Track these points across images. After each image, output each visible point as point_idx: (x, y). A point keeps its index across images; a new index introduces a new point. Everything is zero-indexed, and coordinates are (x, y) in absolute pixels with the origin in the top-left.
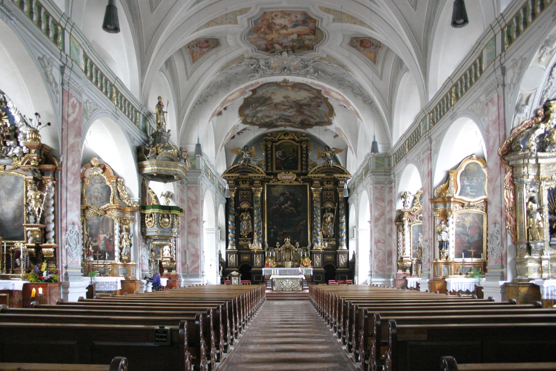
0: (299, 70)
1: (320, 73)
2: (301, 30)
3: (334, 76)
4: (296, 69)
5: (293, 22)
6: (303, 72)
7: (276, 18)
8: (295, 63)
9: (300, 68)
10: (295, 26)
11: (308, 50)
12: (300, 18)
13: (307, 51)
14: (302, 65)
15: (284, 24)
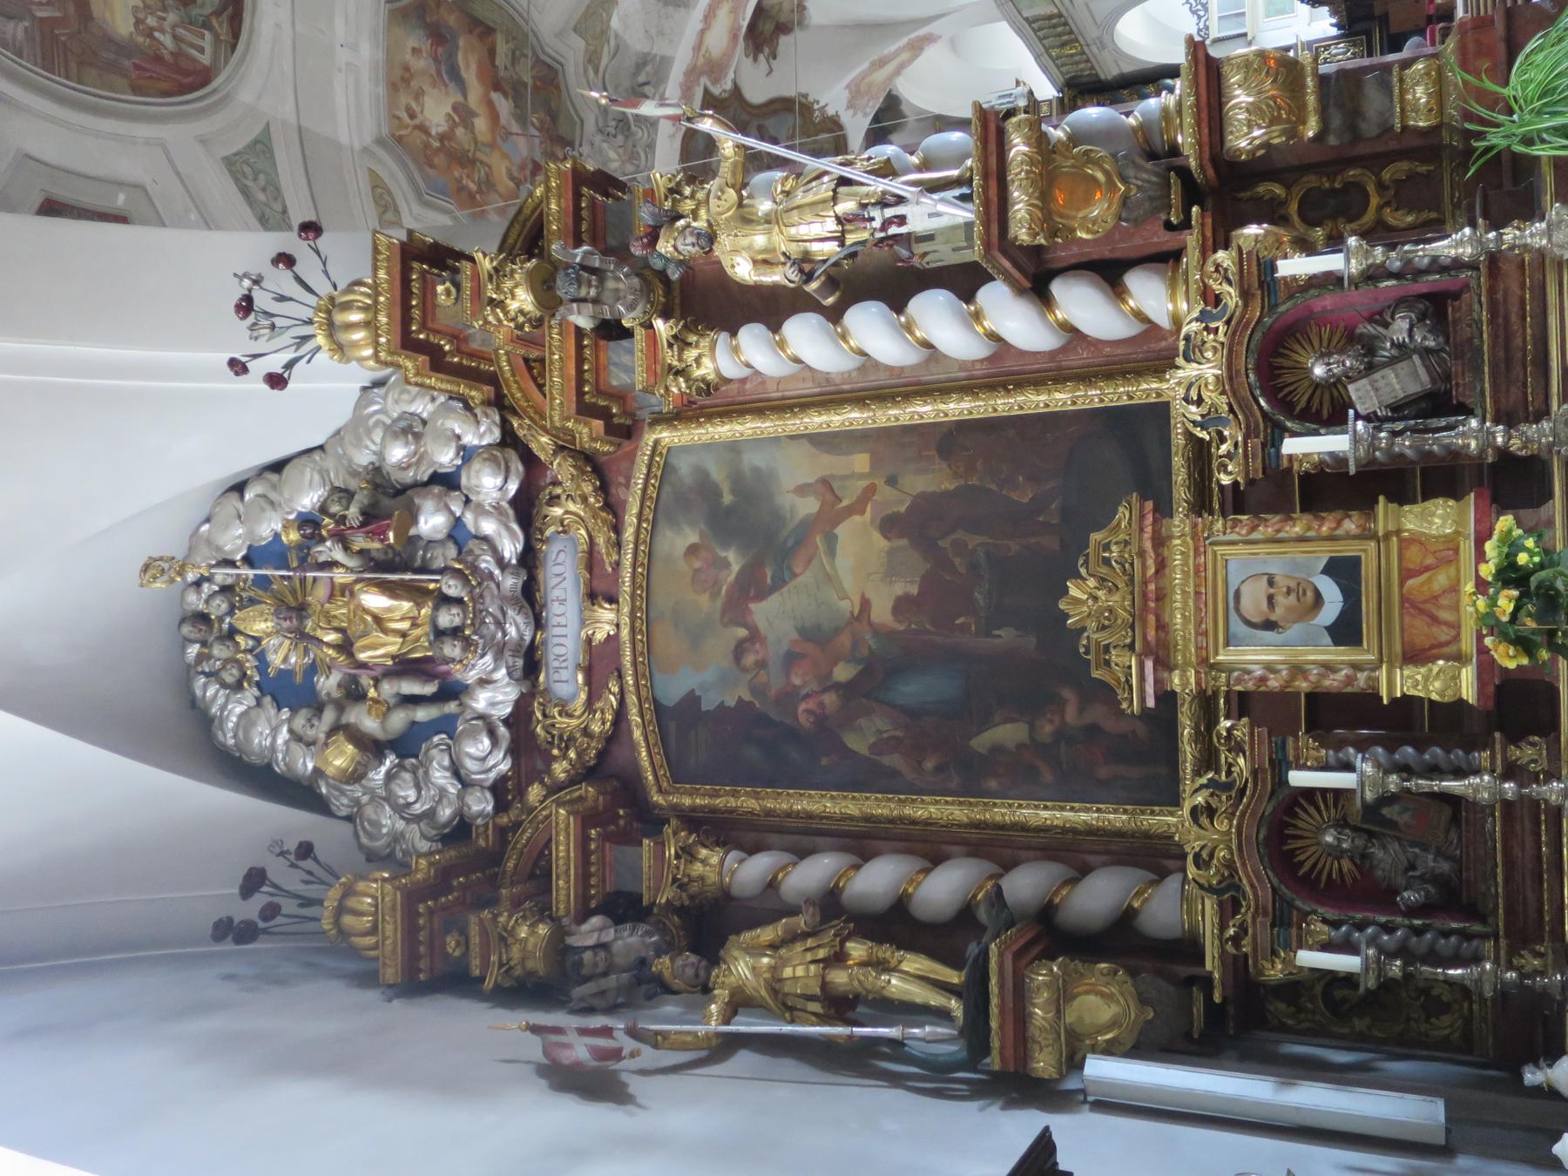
0: (634, 146)
1: (642, 78)
2: (473, 67)
3: (653, 32)
4: (633, 156)
5: (439, 72)
6: (640, 133)
7: (419, 116)
8: (612, 155)
9: (630, 143)
10: (456, 76)
11: (558, 88)
12: (415, 39)
13: (564, 95)
14: (620, 138)
15: (449, 110)
